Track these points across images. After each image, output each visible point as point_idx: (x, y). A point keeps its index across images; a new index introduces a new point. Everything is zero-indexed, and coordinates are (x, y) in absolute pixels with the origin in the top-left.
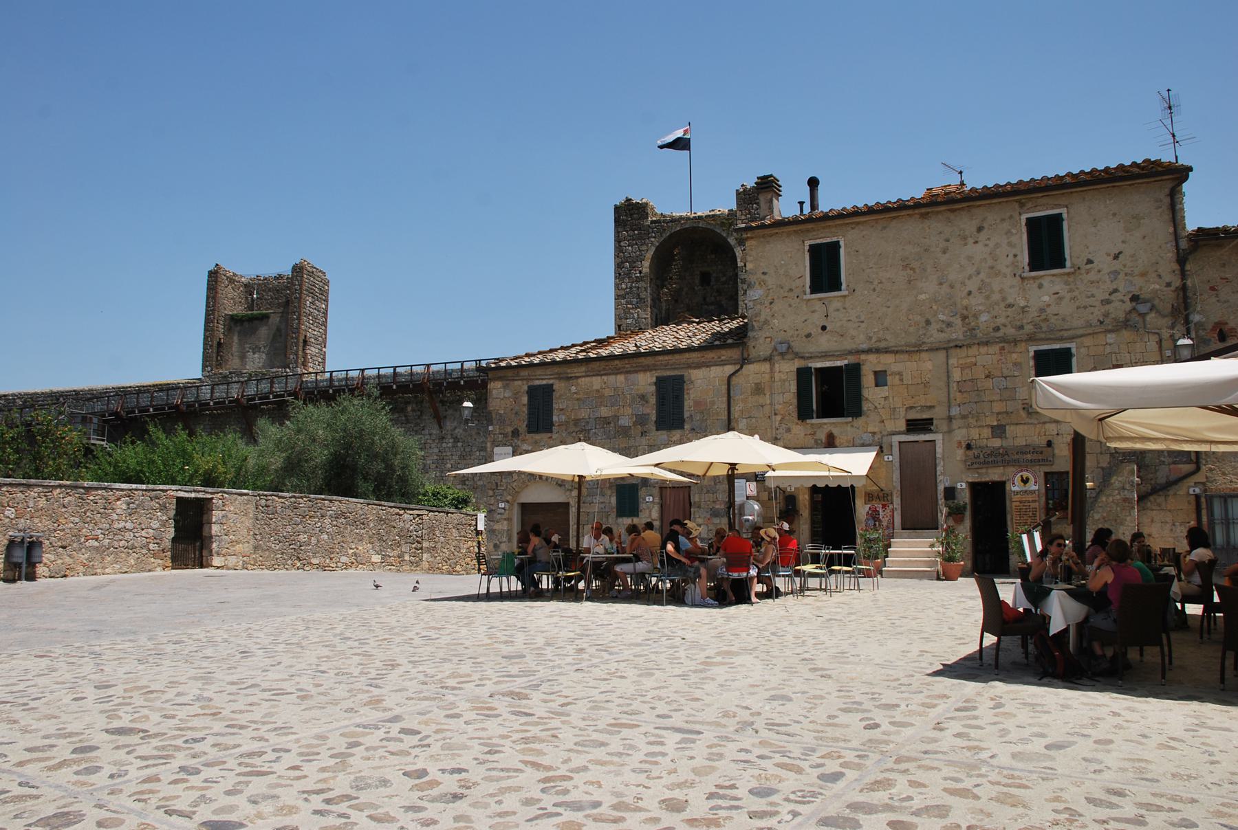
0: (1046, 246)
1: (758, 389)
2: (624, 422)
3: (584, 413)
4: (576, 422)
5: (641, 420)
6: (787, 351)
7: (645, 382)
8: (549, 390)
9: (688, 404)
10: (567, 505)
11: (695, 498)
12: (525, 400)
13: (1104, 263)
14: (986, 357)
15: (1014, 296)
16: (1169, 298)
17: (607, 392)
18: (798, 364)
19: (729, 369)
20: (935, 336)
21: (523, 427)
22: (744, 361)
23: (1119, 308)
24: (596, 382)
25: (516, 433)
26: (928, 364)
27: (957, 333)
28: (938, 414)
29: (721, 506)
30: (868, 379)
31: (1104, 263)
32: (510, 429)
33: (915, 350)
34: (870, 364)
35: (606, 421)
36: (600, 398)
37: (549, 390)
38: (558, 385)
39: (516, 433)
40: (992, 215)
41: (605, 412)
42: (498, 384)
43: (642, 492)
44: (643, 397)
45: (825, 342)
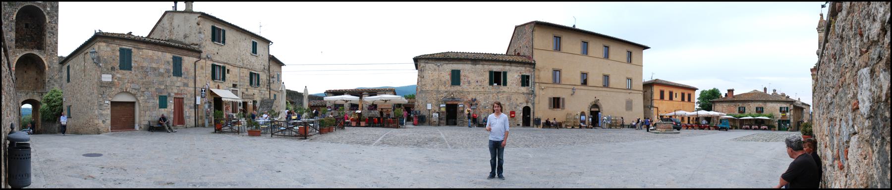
2: (162, 71)
3: (145, 64)
4: (142, 67)
5: (168, 71)
8: (130, 51)
10: (133, 104)
11: (185, 102)
12: (118, 54)
17: (155, 58)
18: (211, 63)
20: (238, 64)
21: (117, 66)
22: (200, 58)
24: (150, 52)
25: (113, 69)
27: (241, 64)
28: (238, 84)
29: (192, 105)
32: (110, 67)
35: (155, 69)
36: (152, 60)
37: (130, 51)
38: (133, 50)
39: (113, 69)
41: (154, 65)
42: (104, 44)
43: (168, 99)
44: (168, 62)
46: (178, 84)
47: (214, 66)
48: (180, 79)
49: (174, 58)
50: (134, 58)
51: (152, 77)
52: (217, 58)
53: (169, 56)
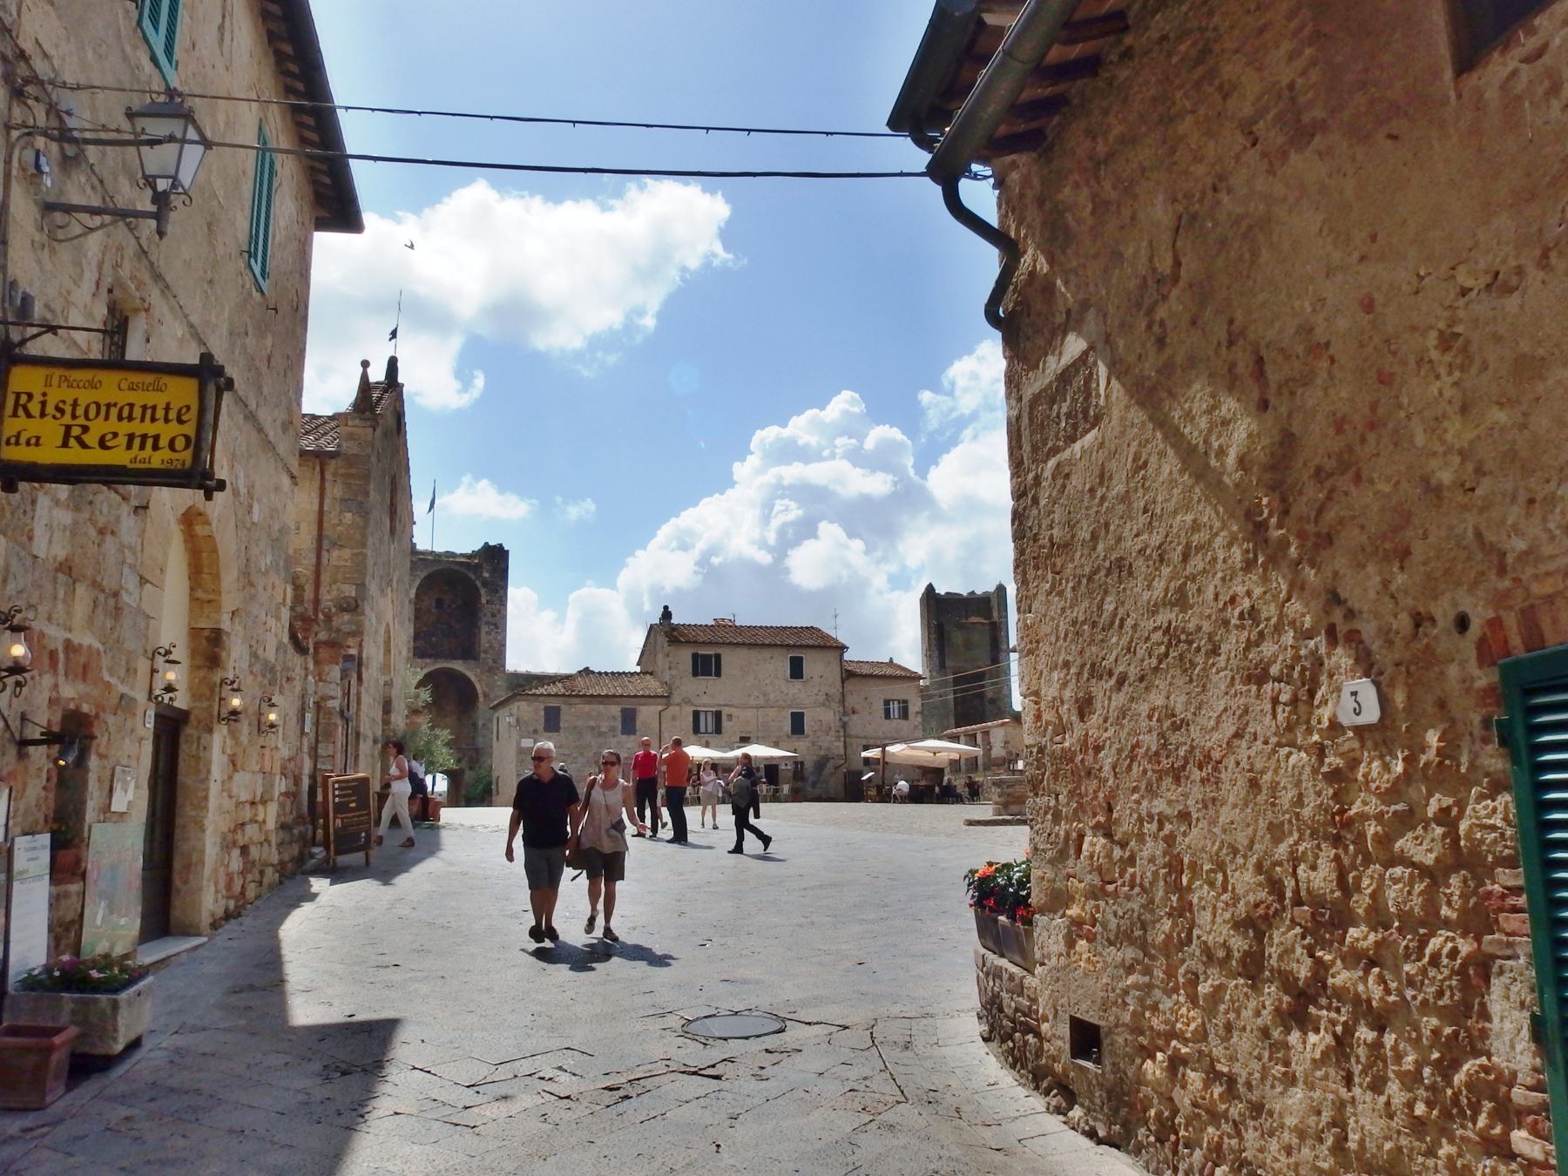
0: (797, 670)
1: (674, 718)
3: (580, 723)
5: (613, 729)
6: (687, 701)
7: (615, 710)
8: (558, 710)
9: (638, 723)
13: (816, 679)
14: (772, 713)
15: (784, 688)
16: (838, 696)
19: (660, 708)
20: (752, 702)
21: (541, 726)
22: (668, 705)
23: (822, 698)
24: (587, 708)
25: (535, 731)
26: (749, 713)
27: (761, 701)
30: (724, 718)
31: (816, 679)
33: (745, 707)
34: (725, 711)
35: (593, 728)
38: (563, 707)
39: (535, 731)
40: (777, 652)
41: (592, 723)
45: (705, 699)
46: (630, 745)
47: (696, 714)
48: (632, 737)
49: (624, 711)
50: (563, 717)
51: (588, 738)
52: (697, 702)
53: (615, 710)
